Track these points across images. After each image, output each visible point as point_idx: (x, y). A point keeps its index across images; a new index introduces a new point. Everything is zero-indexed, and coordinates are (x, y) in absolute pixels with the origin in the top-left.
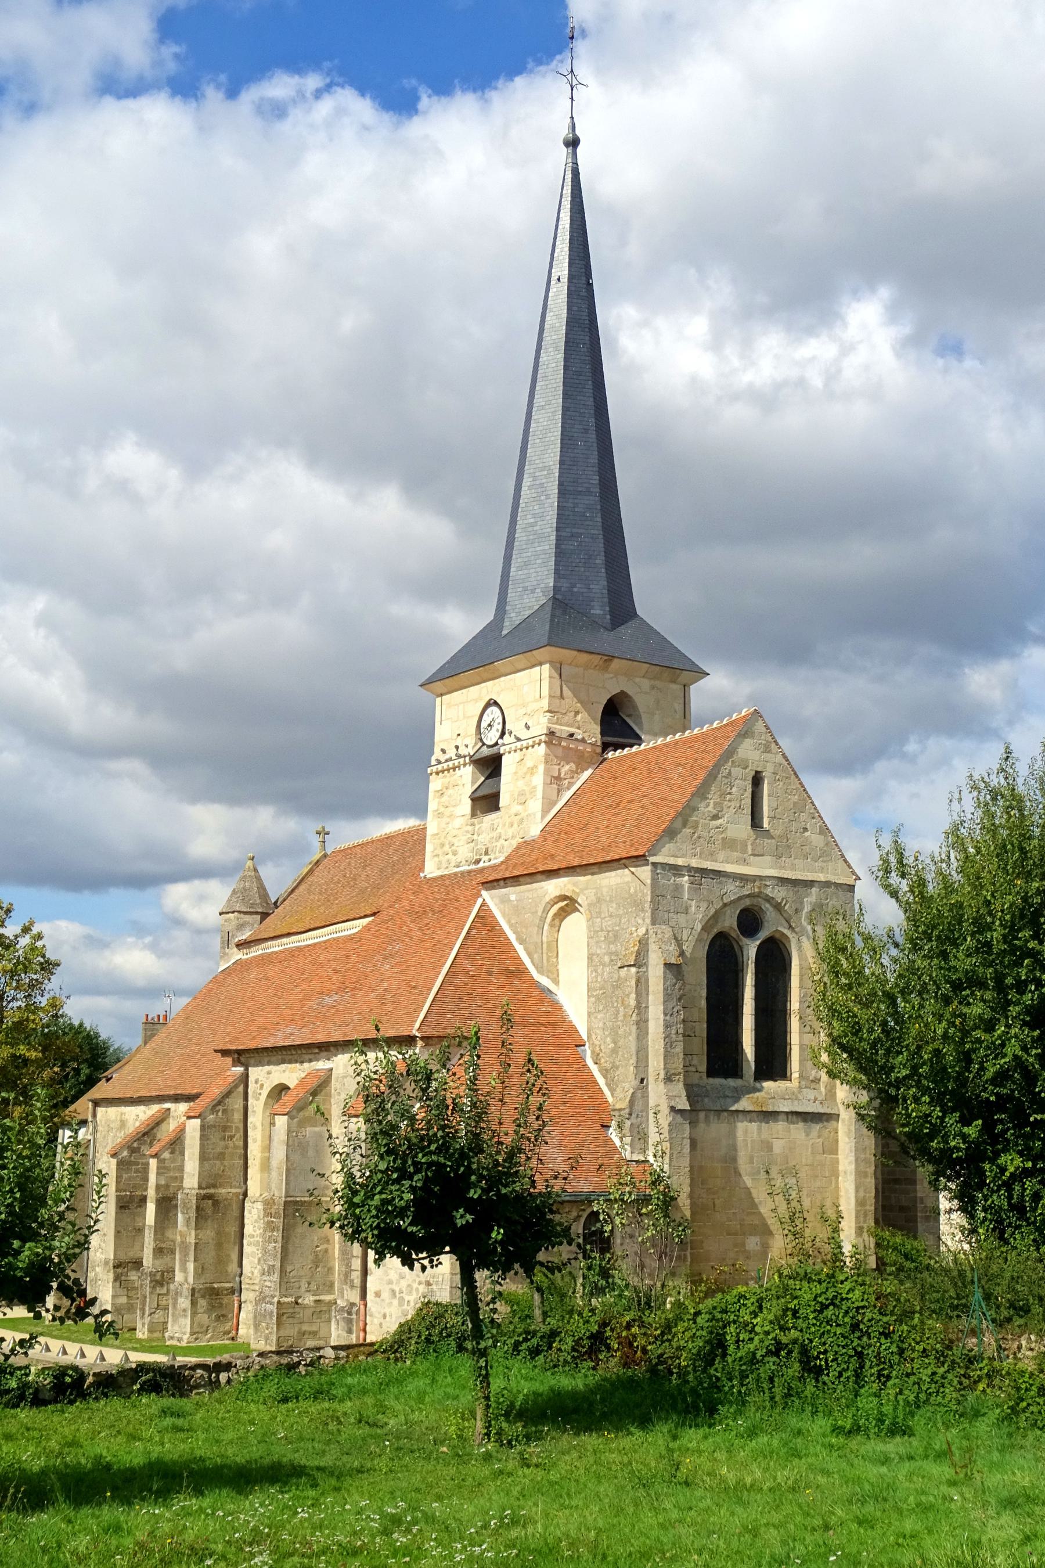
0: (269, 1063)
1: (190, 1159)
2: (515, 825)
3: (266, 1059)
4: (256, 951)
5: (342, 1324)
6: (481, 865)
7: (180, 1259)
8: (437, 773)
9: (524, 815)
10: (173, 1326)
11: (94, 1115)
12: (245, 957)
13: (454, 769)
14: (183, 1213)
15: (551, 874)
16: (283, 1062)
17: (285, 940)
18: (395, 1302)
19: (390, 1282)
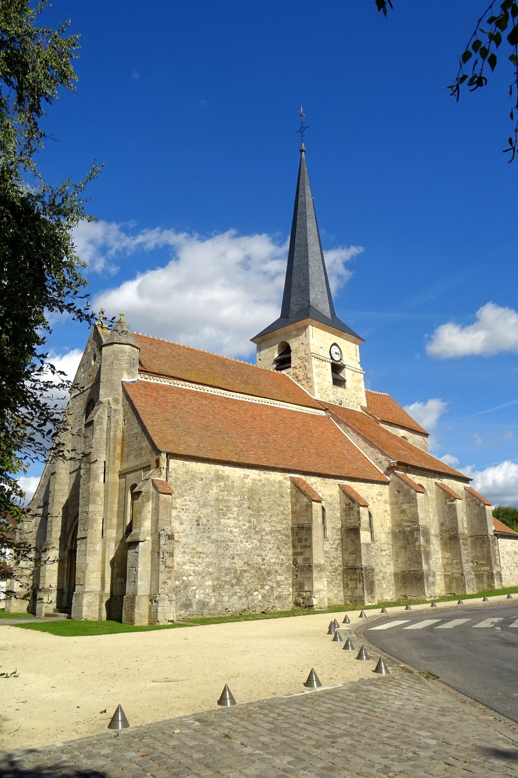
0: (414, 474)
1: (421, 512)
2: (354, 398)
3: (413, 472)
4: (154, 380)
5: (498, 579)
6: (342, 406)
7: (425, 559)
8: (315, 358)
9: (357, 396)
10: (428, 591)
11: (168, 464)
12: (143, 379)
13: (323, 361)
14: (423, 537)
15: (403, 427)
16: (420, 475)
17: (208, 388)
18: (508, 570)
19: (505, 564)
